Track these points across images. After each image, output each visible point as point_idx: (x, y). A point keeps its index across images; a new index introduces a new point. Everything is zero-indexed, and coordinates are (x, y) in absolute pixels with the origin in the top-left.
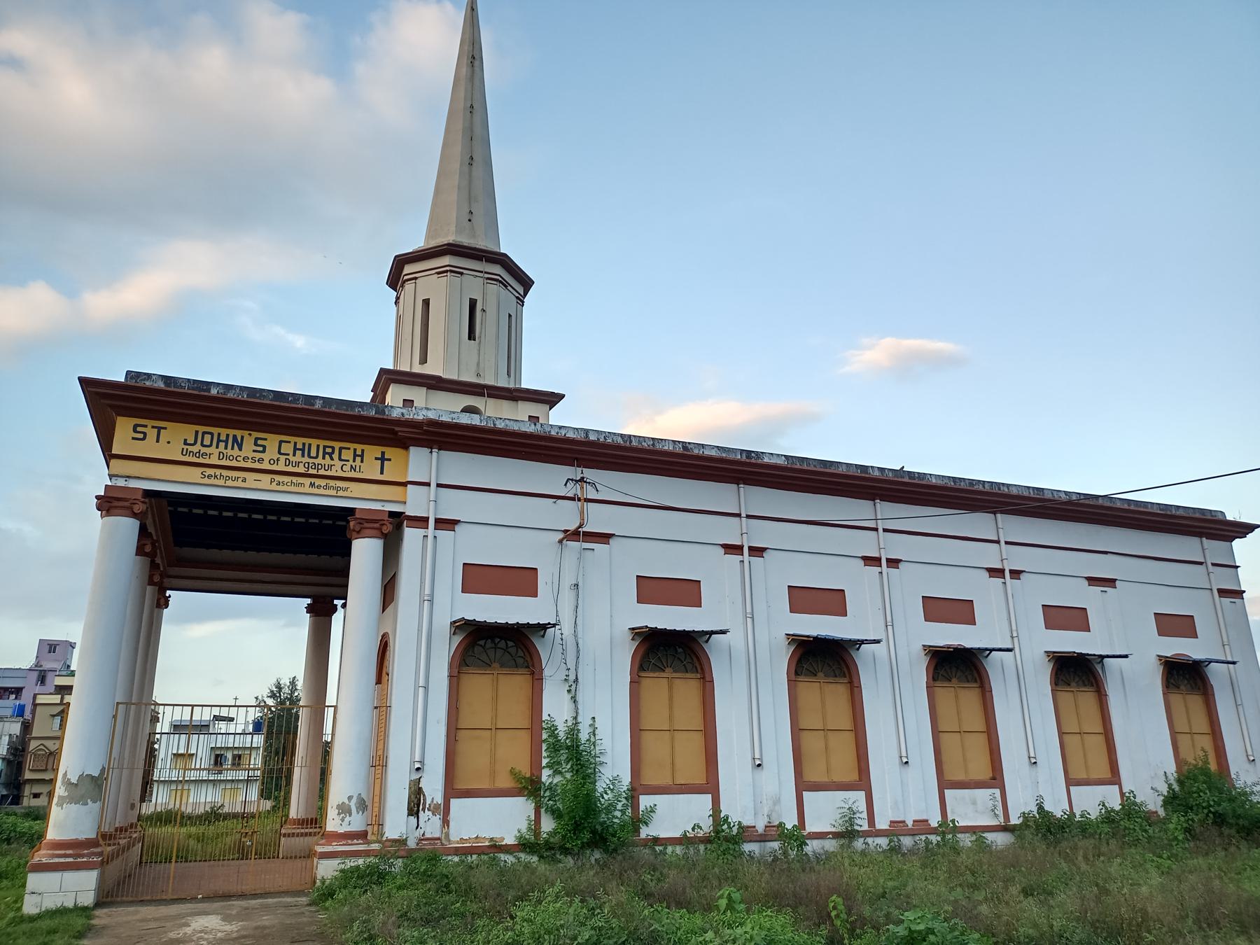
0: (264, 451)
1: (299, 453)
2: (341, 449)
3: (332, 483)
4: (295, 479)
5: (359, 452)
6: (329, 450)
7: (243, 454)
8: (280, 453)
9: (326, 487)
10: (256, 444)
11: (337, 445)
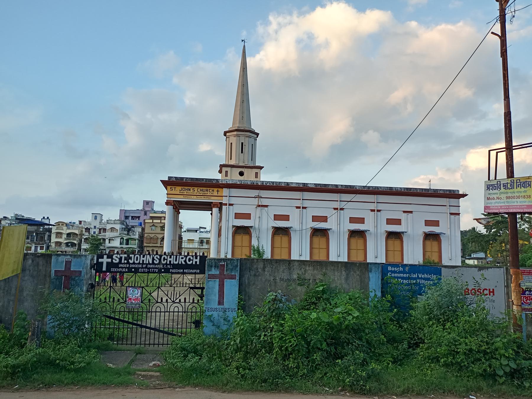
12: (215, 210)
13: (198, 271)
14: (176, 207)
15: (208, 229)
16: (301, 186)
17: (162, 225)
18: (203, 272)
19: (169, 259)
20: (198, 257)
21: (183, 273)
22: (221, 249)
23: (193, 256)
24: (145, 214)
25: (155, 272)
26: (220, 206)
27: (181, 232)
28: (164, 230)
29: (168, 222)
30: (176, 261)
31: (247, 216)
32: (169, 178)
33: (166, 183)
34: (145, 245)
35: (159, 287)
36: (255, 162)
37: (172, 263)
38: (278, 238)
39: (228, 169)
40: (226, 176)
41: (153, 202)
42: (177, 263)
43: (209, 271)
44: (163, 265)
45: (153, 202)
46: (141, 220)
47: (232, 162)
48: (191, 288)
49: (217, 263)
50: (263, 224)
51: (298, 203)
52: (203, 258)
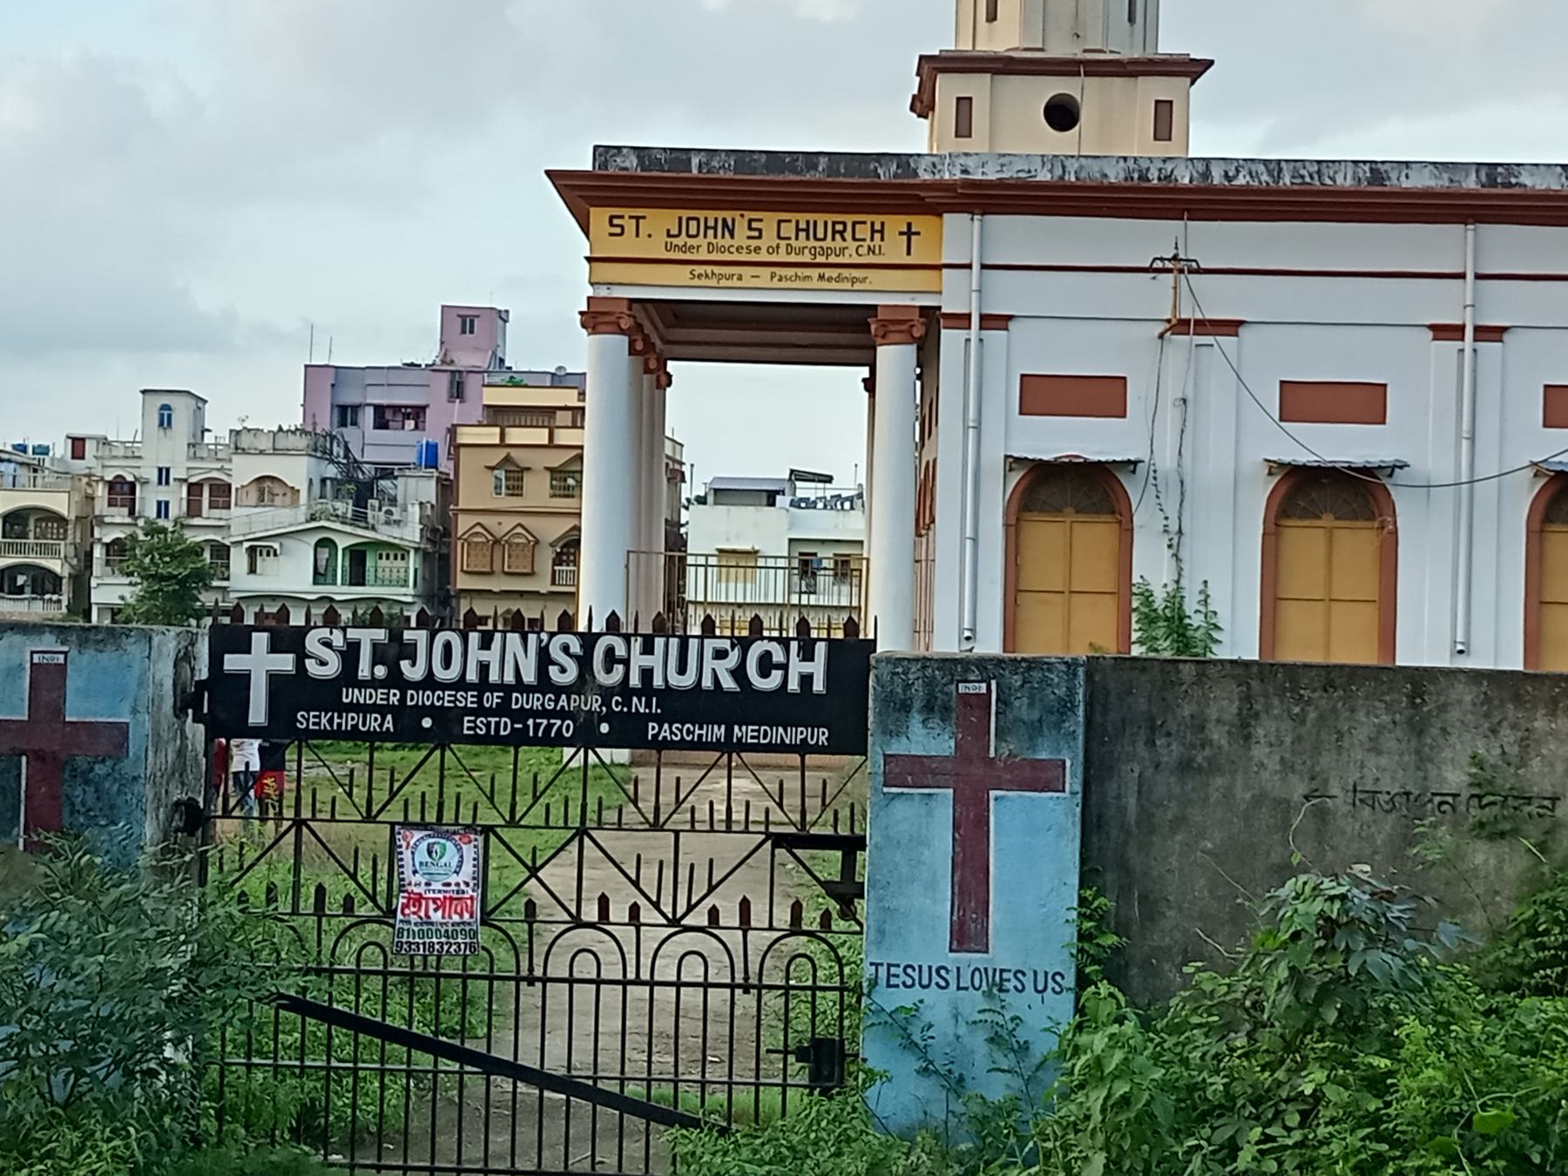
0: (760, 237)
1: (802, 235)
2: (854, 224)
3: (846, 272)
4: (800, 271)
5: (878, 227)
6: (839, 227)
7: (736, 243)
8: (779, 237)
9: (839, 279)
10: (750, 228)
11: (849, 219)
12: (894, 359)
13: (822, 736)
14: (649, 345)
15: (845, 484)
16: (1471, 183)
17: (557, 459)
18: (850, 740)
19: (638, 661)
20: (821, 649)
21: (729, 747)
22: (945, 602)
23: (784, 642)
24: (458, 391)
25: (560, 741)
26: (924, 331)
27: (677, 505)
28: (573, 492)
29: (598, 442)
30: (682, 670)
31: (1102, 396)
32: (603, 153)
33: (585, 192)
34: (463, 582)
35: (582, 832)
36: (1151, 32)
37: (658, 682)
38: (1306, 539)
39: (976, 86)
40: (963, 129)
41: (503, 316)
42: (688, 681)
43: (889, 733)
44: (606, 693)
45: (503, 316)
46: (434, 430)
47: (1003, 39)
48: (779, 841)
49: (939, 685)
50: (1206, 449)
51: (1448, 304)
52: (852, 652)
